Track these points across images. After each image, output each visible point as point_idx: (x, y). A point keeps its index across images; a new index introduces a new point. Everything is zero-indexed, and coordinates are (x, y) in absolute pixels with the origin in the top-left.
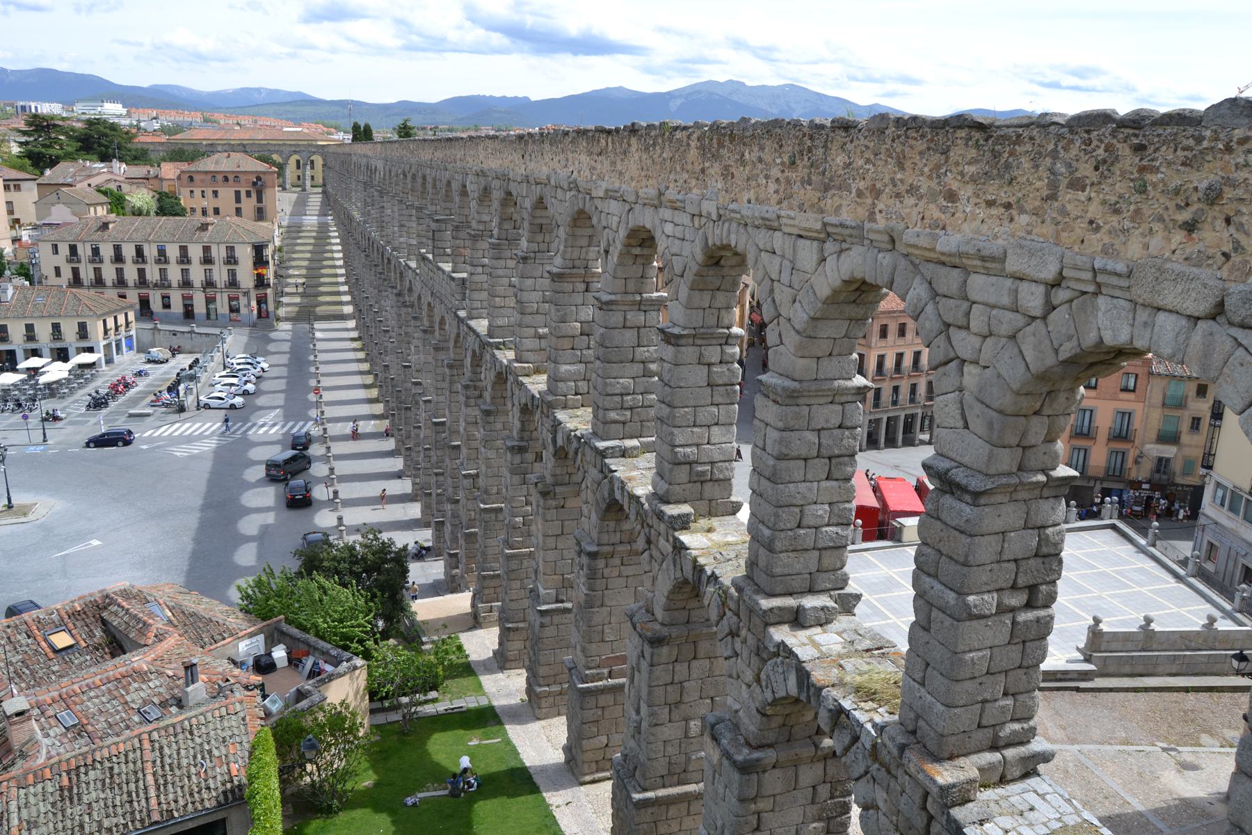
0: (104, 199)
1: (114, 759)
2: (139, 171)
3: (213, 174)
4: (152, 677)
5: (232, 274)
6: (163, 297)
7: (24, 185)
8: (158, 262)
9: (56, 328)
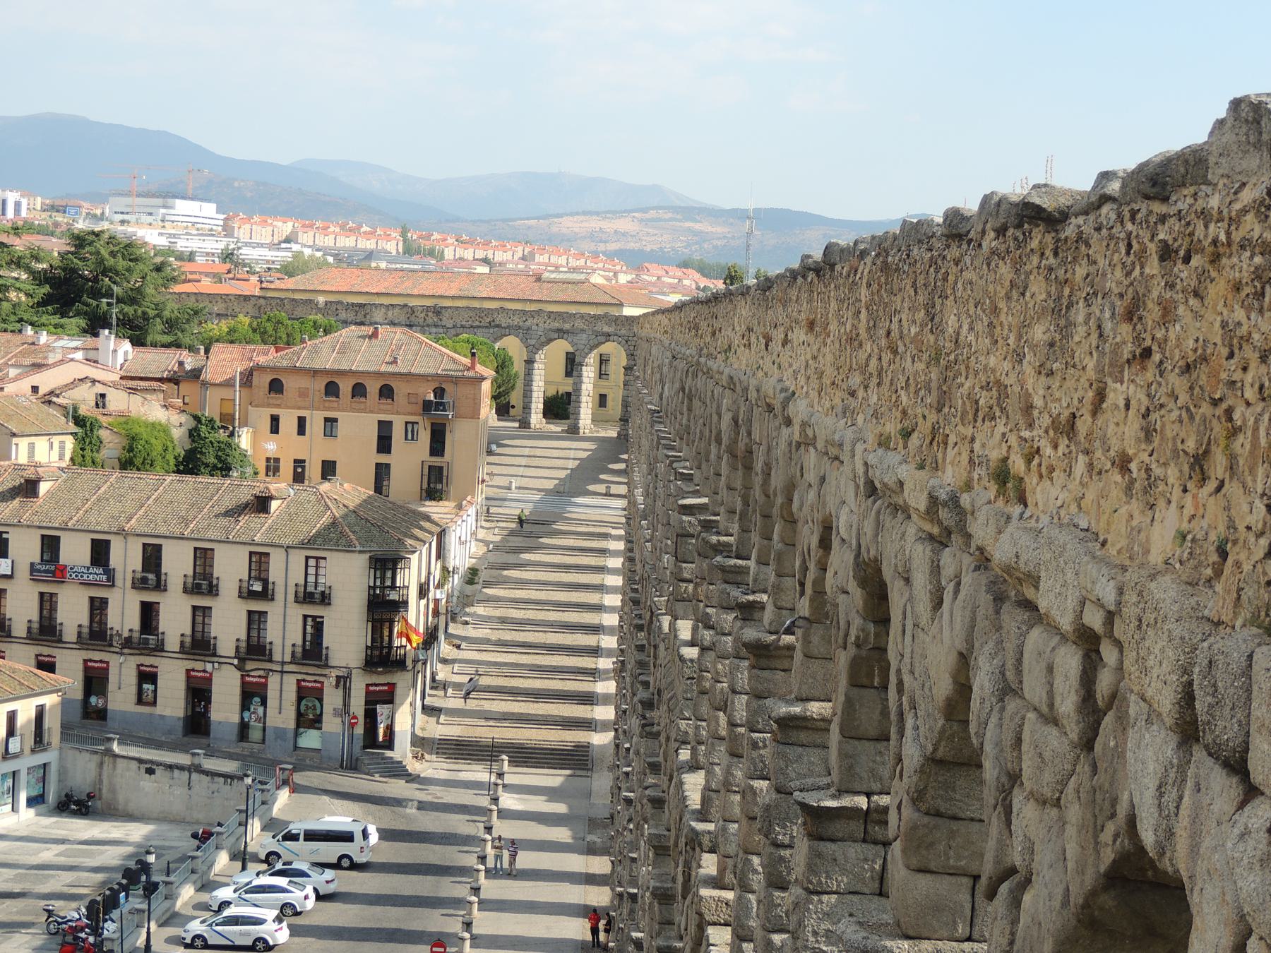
2: (161, 361)
8: (140, 584)
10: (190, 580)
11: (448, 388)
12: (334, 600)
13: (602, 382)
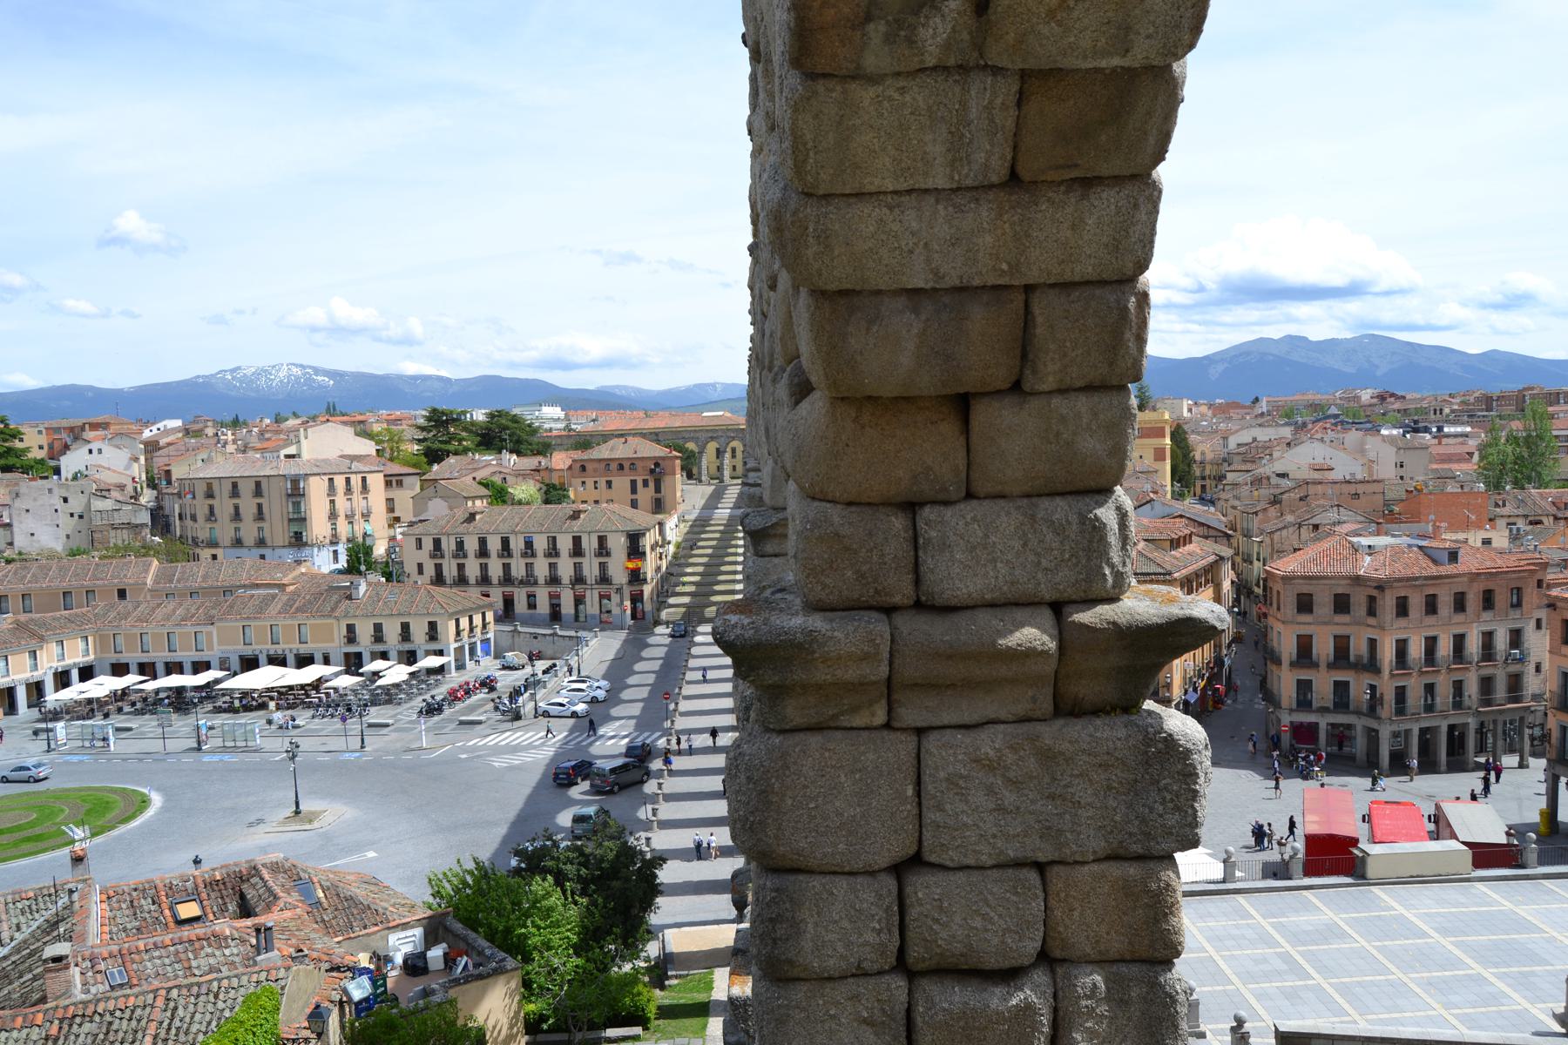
0: (485, 492)
1: (118, 1013)
2: (530, 462)
3: (607, 462)
4: (232, 944)
5: (603, 566)
7: (407, 480)
8: (524, 555)
9: (405, 627)
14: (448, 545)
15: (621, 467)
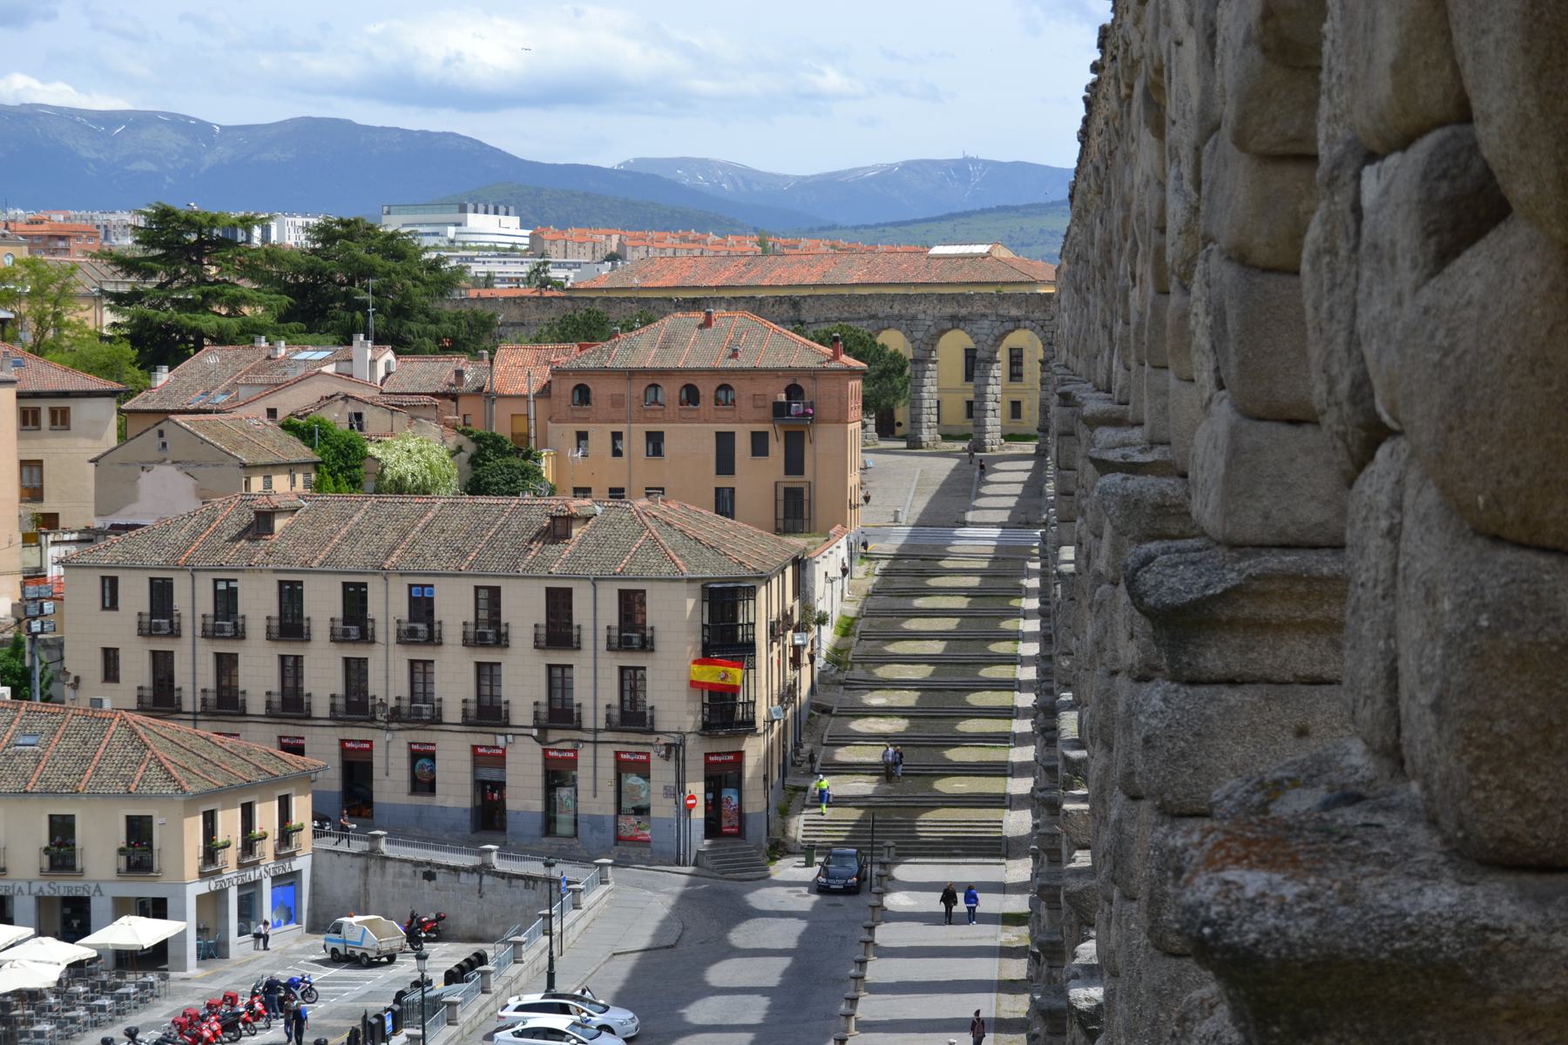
0: (299, 451)
2: (432, 372)
3: (653, 378)
5: (631, 680)
6: (415, 756)
7: (81, 411)
8: (407, 637)
10: (471, 629)
11: (803, 383)
12: (658, 646)
13: (1016, 386)
14: (193, 600)
15: (691, 395)
